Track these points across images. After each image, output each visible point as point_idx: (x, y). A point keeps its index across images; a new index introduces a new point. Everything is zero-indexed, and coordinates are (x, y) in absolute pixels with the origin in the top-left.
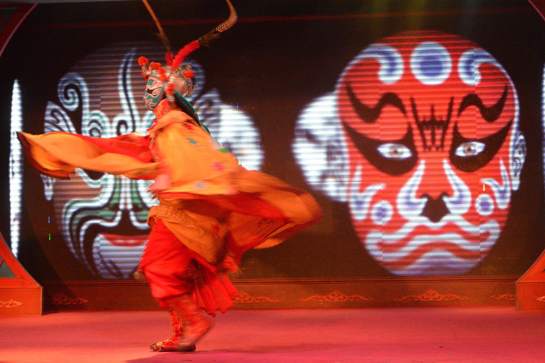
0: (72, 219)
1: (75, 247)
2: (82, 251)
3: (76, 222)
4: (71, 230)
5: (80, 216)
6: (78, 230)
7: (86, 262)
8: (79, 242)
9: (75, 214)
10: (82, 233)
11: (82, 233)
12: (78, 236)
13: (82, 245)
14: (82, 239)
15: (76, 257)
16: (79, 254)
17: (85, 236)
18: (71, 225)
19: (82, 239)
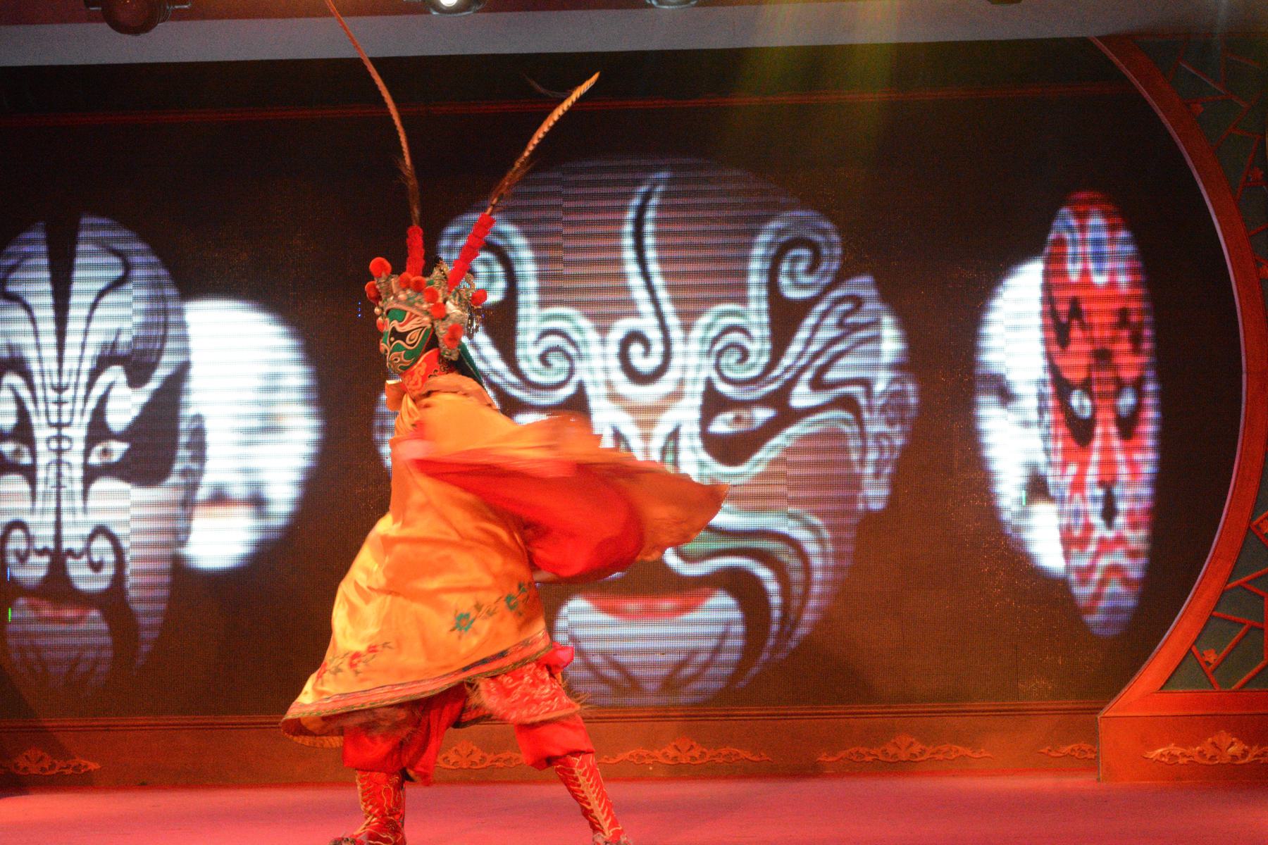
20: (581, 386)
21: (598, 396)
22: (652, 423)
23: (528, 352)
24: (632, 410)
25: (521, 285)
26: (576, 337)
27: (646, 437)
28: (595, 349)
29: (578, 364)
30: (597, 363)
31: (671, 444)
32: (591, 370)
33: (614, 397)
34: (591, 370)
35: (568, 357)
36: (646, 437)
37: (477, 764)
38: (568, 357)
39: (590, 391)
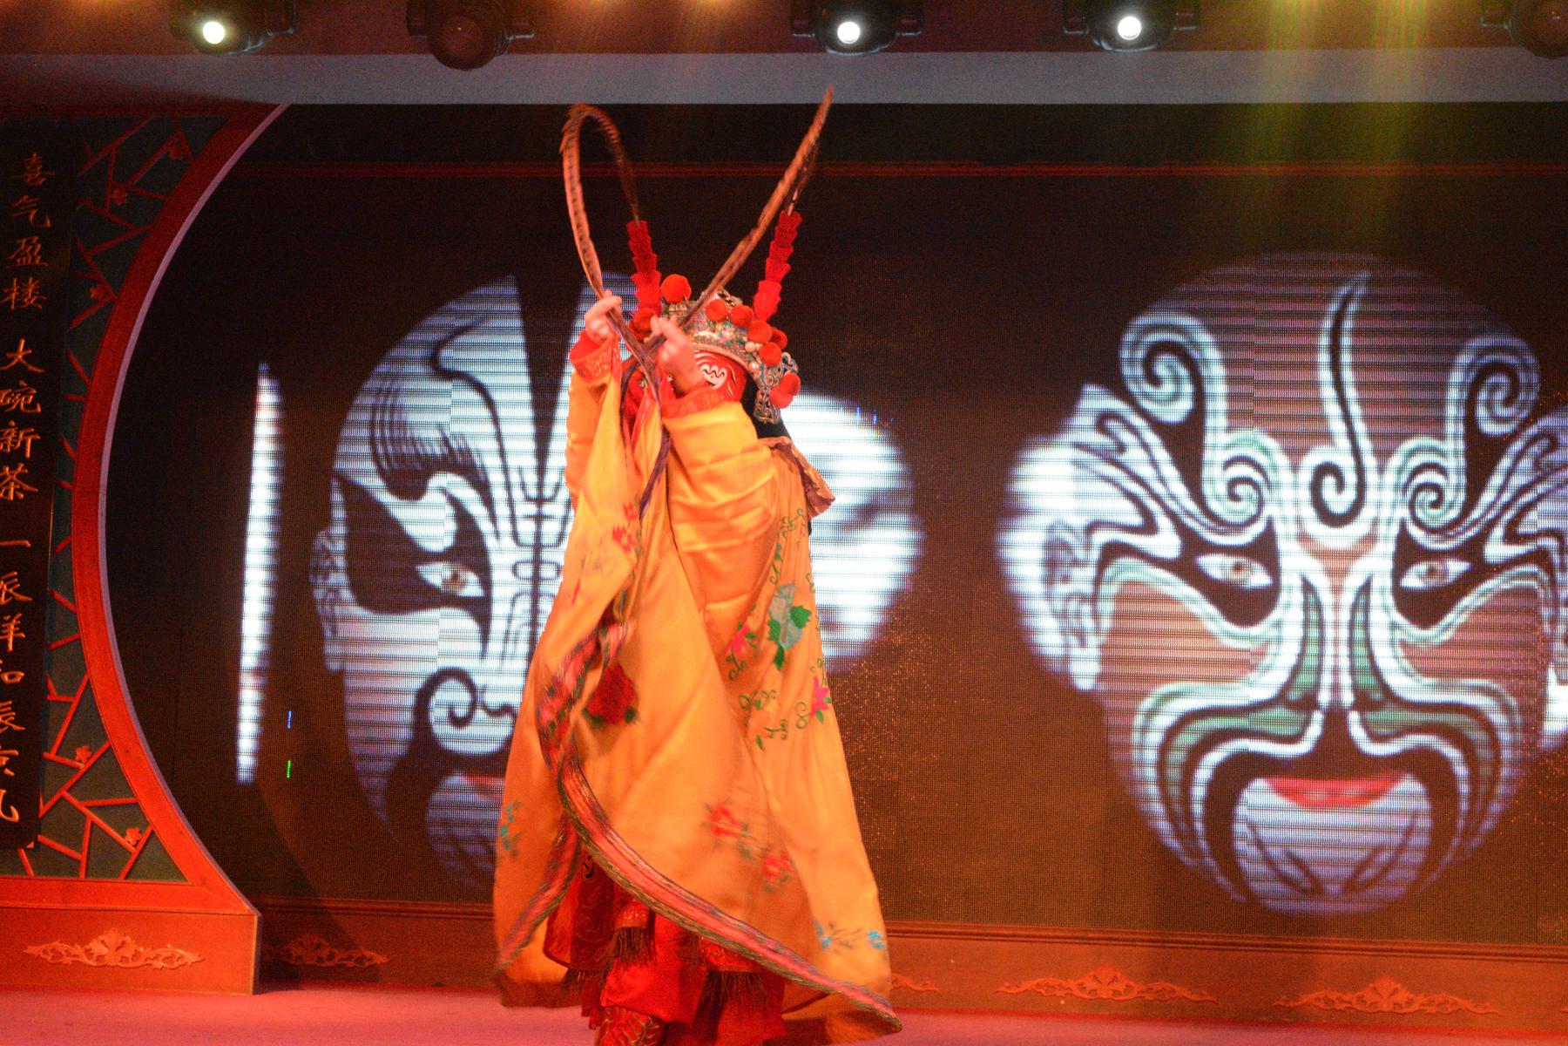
0: (1164, 749)
1: (1179, 835)
2: (1203, 844)
3: (1177, 756)
4: (1162, 782)
5: (1187, 739)
6: (1187, 781)
7: (1221, 879)
8: (1189, 816)
9: (1172, 733)
10: (1199, 792)
11: (1199, 792)
12: (1186, 799)
13: (1199, 826)
14: (1198, 809)
15: (1186, 860)
16: (1195, 853)
17: (1208, 802)
18: (1161, 765)
19: (1198, 809)
20: (1270, 523)
21: (1287, 536)
22: (1344, 573)
23: (1215, 479)
24: (1321, 554)
25: (1209, 389)
26: (1262, 459)
27: (1337, 590)
28: (1285, 476)
29: (1266, 493)
30: (1286, 494)
31: (1362, 601)
32: (1280, 503)
33: (1303, 538)
34: (1280, 503)
35: (1255, 485)
36: (1337, 590)
37: (1402, 1008)
38: (1255, 485)
39: (1279, 528)
